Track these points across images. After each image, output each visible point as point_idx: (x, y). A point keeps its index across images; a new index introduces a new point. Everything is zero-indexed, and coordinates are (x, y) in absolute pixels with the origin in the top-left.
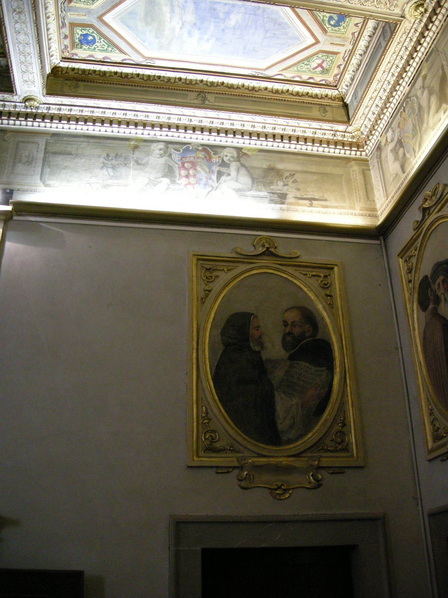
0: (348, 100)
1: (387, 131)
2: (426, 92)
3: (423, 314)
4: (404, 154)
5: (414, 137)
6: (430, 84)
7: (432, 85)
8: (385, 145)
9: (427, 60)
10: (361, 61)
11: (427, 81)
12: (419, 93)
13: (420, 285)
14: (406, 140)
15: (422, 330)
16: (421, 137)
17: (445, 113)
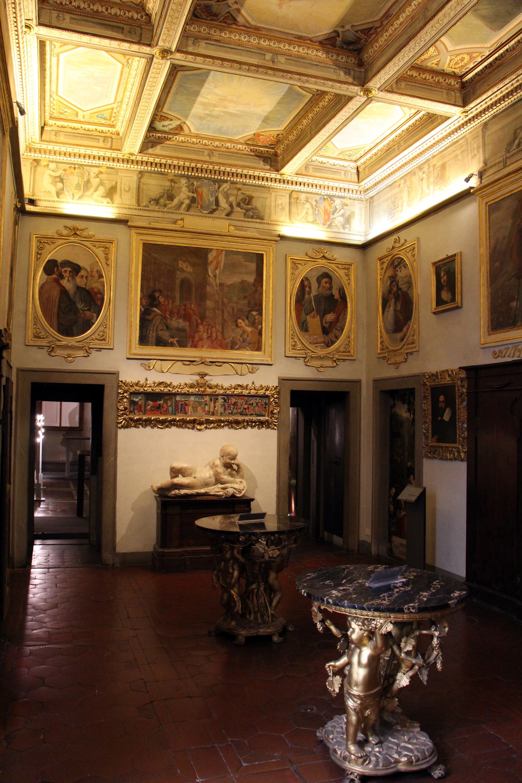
0: (46, 128)
1: (52, 162)
2: (97, 180)
3: (45, 276)
4: (63, 189)
5: (76, 189)
6: (104, 180)
7: (104, 181)
8: (45, 166)
9: (107, 168)
10: (78, 129)
11: (102, 176)
12: (92, 174)
13: (48, 261)
14: (68, 184)
15: (42, 283)
16: (83, 195)
17: (108, 203)
